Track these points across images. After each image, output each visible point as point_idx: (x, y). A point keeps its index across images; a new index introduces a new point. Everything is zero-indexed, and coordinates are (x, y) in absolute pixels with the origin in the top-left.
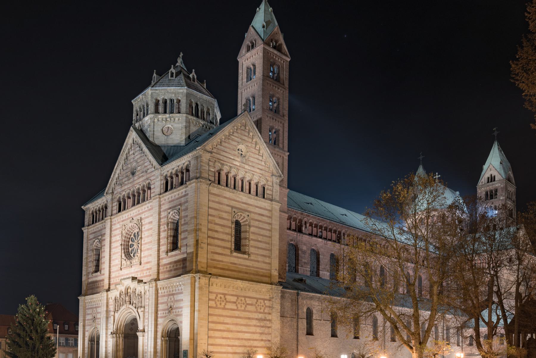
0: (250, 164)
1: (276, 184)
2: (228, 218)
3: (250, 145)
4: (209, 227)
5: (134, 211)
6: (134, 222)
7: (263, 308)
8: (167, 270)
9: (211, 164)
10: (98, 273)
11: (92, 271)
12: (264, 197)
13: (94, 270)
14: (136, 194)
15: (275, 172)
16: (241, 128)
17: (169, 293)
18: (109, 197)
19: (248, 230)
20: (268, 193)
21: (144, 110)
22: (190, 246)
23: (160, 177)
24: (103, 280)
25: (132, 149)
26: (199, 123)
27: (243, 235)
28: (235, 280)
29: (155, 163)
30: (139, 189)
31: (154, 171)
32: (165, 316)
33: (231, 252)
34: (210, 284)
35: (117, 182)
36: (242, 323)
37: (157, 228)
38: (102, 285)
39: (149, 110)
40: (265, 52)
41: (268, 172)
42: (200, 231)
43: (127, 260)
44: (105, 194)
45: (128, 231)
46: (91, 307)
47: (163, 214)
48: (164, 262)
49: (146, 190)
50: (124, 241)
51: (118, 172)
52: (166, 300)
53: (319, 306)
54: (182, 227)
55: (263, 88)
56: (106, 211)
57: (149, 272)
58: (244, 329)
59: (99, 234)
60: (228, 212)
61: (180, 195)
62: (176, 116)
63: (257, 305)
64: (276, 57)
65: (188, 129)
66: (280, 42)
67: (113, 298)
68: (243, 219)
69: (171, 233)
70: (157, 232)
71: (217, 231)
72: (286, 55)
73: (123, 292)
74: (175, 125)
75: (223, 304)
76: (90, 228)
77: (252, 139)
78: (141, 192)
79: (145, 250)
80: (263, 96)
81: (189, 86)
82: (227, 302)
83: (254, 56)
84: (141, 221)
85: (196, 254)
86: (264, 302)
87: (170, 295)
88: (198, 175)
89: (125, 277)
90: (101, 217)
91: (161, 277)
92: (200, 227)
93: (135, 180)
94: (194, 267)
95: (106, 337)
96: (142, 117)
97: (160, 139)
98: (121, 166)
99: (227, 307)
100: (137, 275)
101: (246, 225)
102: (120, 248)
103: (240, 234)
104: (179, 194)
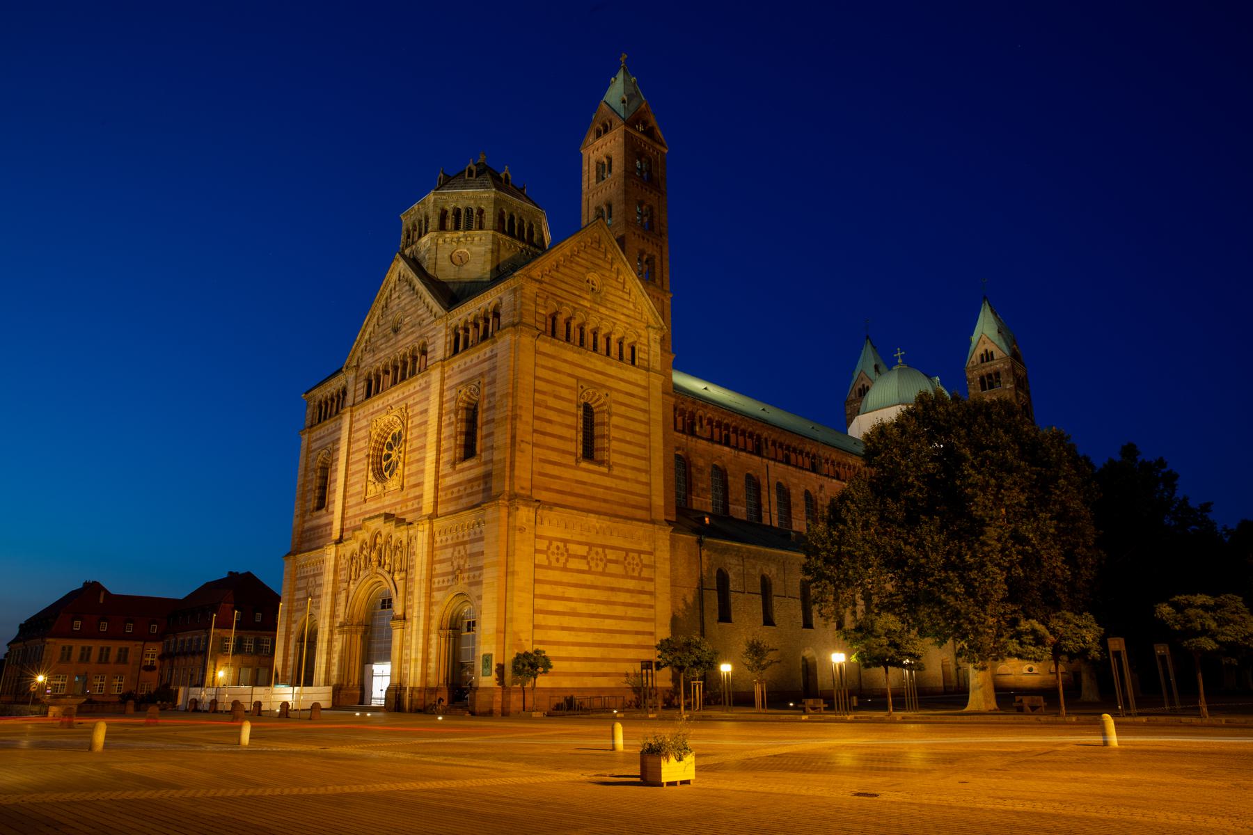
0: (609, 306)
1: (655, 342)
2: (569, 397)
3: (607, 274)
4: (536, 413)
5: (395, 395)
6: (394, 414)
7: (637, 569)
8: (454, 496)
9: (539, 301)
10: (324, 511)
11: (311, 507)
12: (633, 363)
13: (315, 505)
14: (399, 364)
15: (652, 321)
16: (593, 246)
17: (455, 541)
18: (351, 375)
19: (606, 420)
20: (641, 356)
21: (420, 229)
22: (498, 448)
23: (444, 331)
24: (331, 523)
25: (397, 289)
26: (516, 246)
27: (597, 431)
28: (585, 514)
29: (437, 307)
30: (405, 355)
31: (432, 322)
32: (448, 587)
33: (577, 461)
34: (538, 520)
35: (366, 347)
36: (599, 598)
37: (437, 419)
38: (329, 532)
39: (430, 225)
40: (628, 138)
41: (641, 321)
42: (518, 420)
43: (377, 483)
44: (344, 370)
45: (382, 430)
46: (305, 574)
47: (447, 395)
48: (448, 481)
49: (418, 355)
50: (374, 449)
51: (370, 329)
52: (449, 555)
53: (739, 565)
54: (485, 415)
55: (625, 191)
56: (344, 399)
57: (418, 503)
58: (602, 609)
59: (329, 441)
60: (571, 388)
61: (482, 358)
62: (477, 234)
63: (626, 562)
64: (645, 145)
65: (496, 254)
66: (650, 125)
67: (348, 555)
68: (598, 400)
69: (462, 427)
70: (436, 428)
71: (550, 421)
72: (662, 144)
73: (366, 544)
74: (474, 249)
75: (562, 560)
76: (315, 431)
77: (612, 264)
78: (409, 360)
79: (412, 463)
80: (626, 202)
81: (499, 188)
82: (569, 556)
83: (608, 144)
84: (406, 410)
85: (511, 463)
86: (639, 557)
87: (457, 544)
88: (516, 320)
89: (372, 515)
90: (335, 410)
91: (440, 510)
92: (518, 412)
93: (399, 341)
94: (507, 488)
95: (331, 632)
96: (416, 238)
97: (447, 272)
98: (375, 320)
99: (569, 565)
100: (396, 509)
101: (603, 412)
102: (366, 462)
103: (592, 429)
104: (479, 357)
